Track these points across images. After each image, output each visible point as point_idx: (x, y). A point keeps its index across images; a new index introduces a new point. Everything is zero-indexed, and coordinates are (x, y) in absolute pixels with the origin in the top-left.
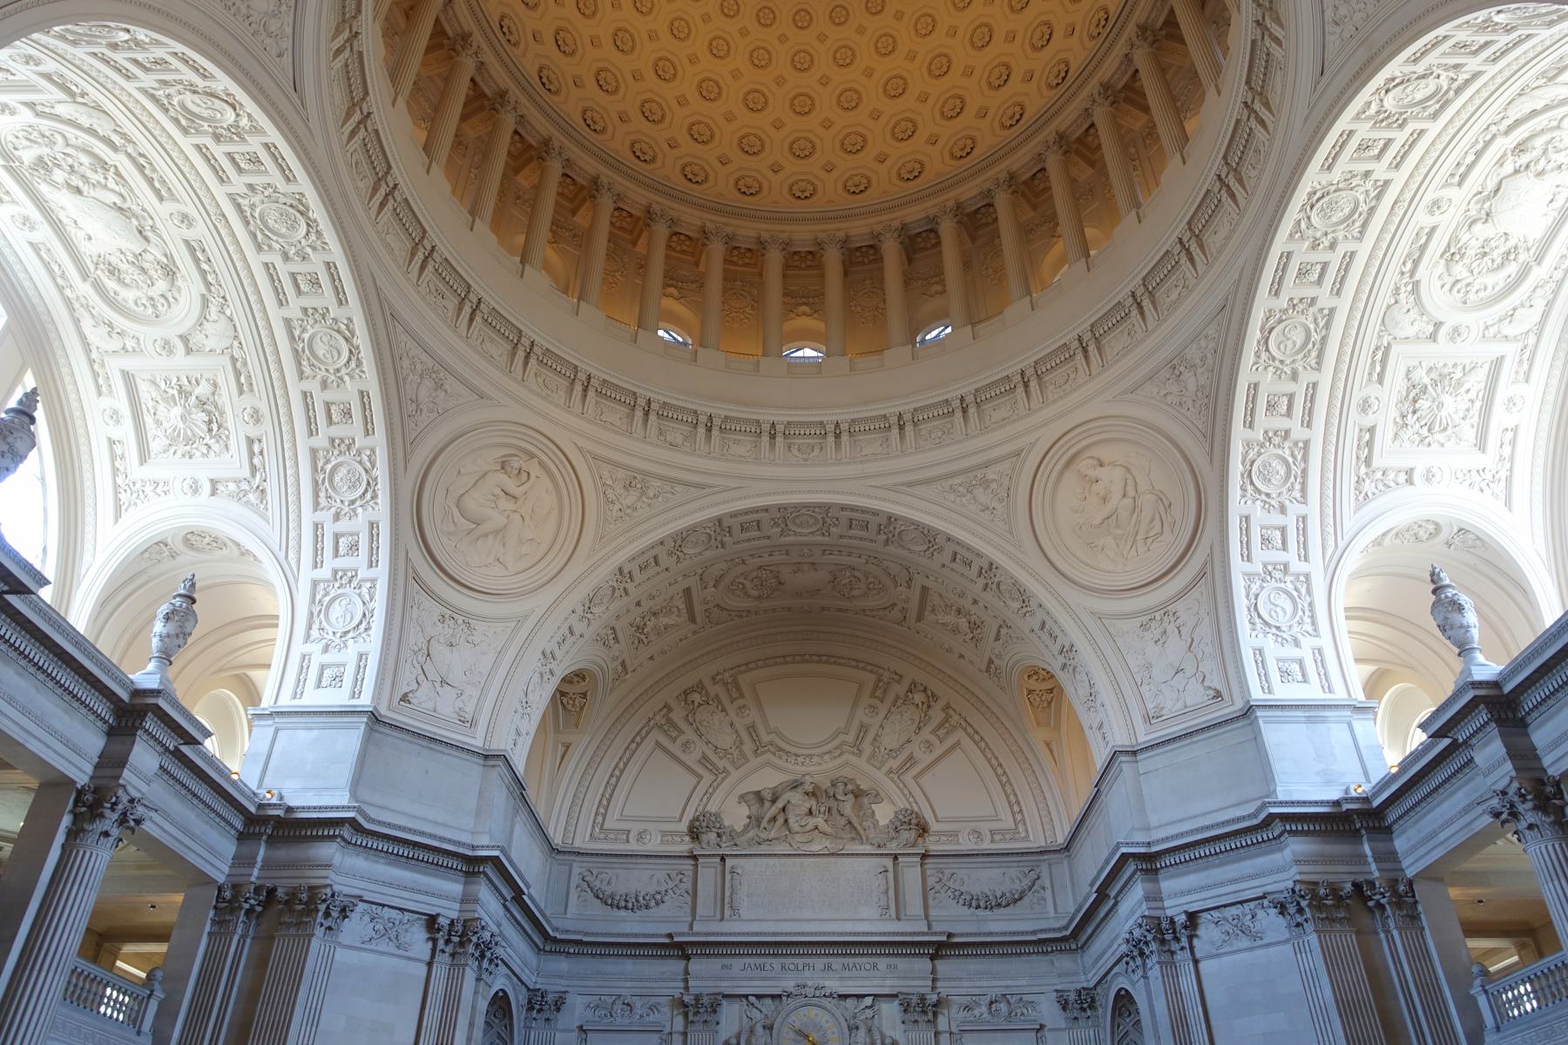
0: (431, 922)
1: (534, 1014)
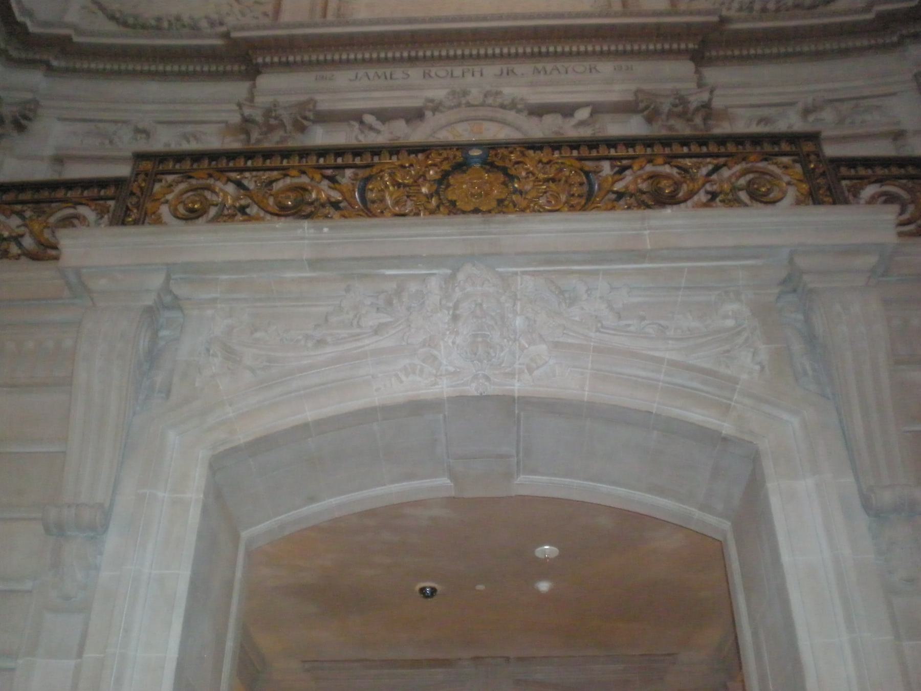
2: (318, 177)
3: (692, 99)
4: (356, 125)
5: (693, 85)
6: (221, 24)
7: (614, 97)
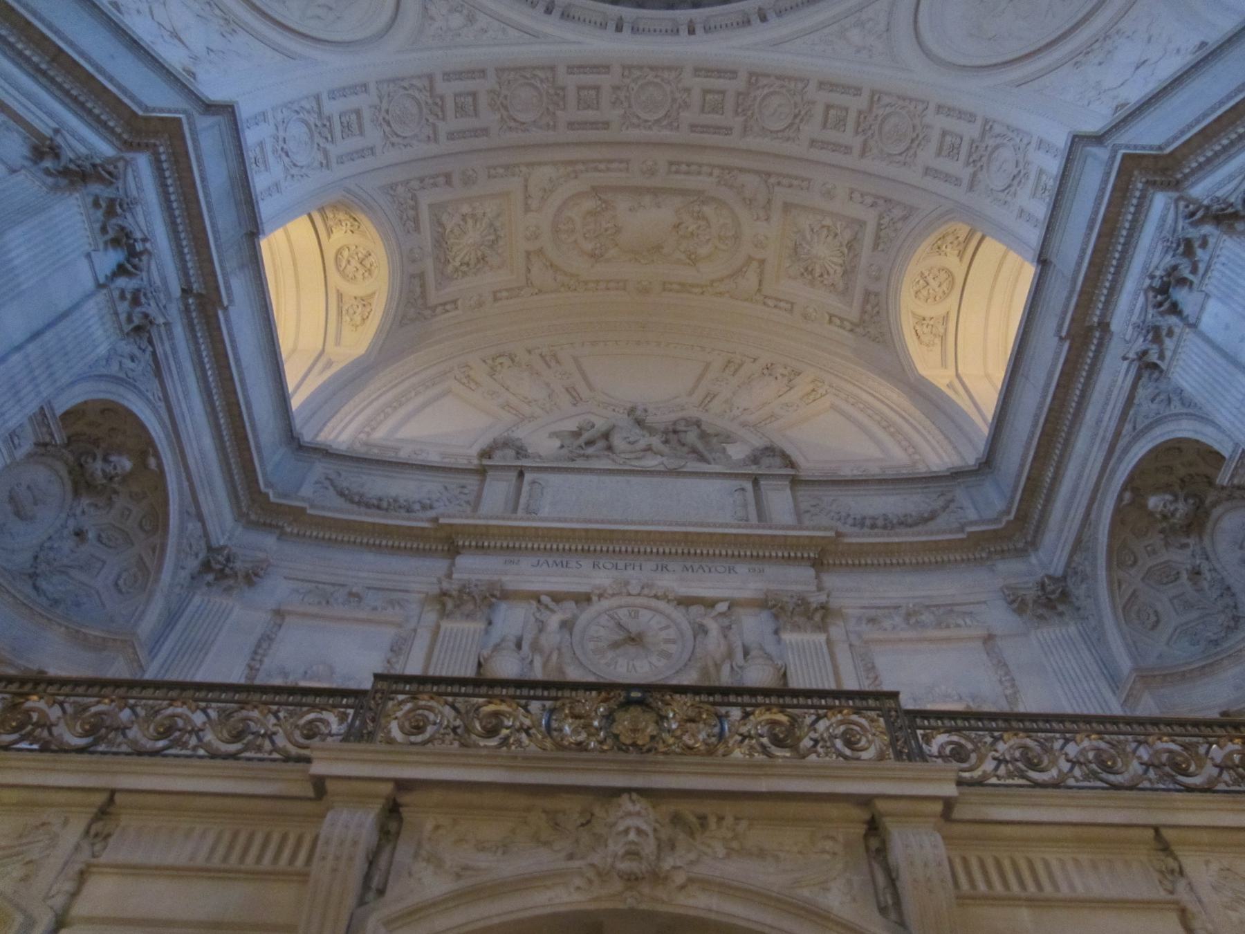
0: (43, 150)
1: (210, 577)
2: (514, 705)
3: (812, 600)
4: (534, 603)
5: (814, 588)
6: (431, 507)
7: (747, 594)
